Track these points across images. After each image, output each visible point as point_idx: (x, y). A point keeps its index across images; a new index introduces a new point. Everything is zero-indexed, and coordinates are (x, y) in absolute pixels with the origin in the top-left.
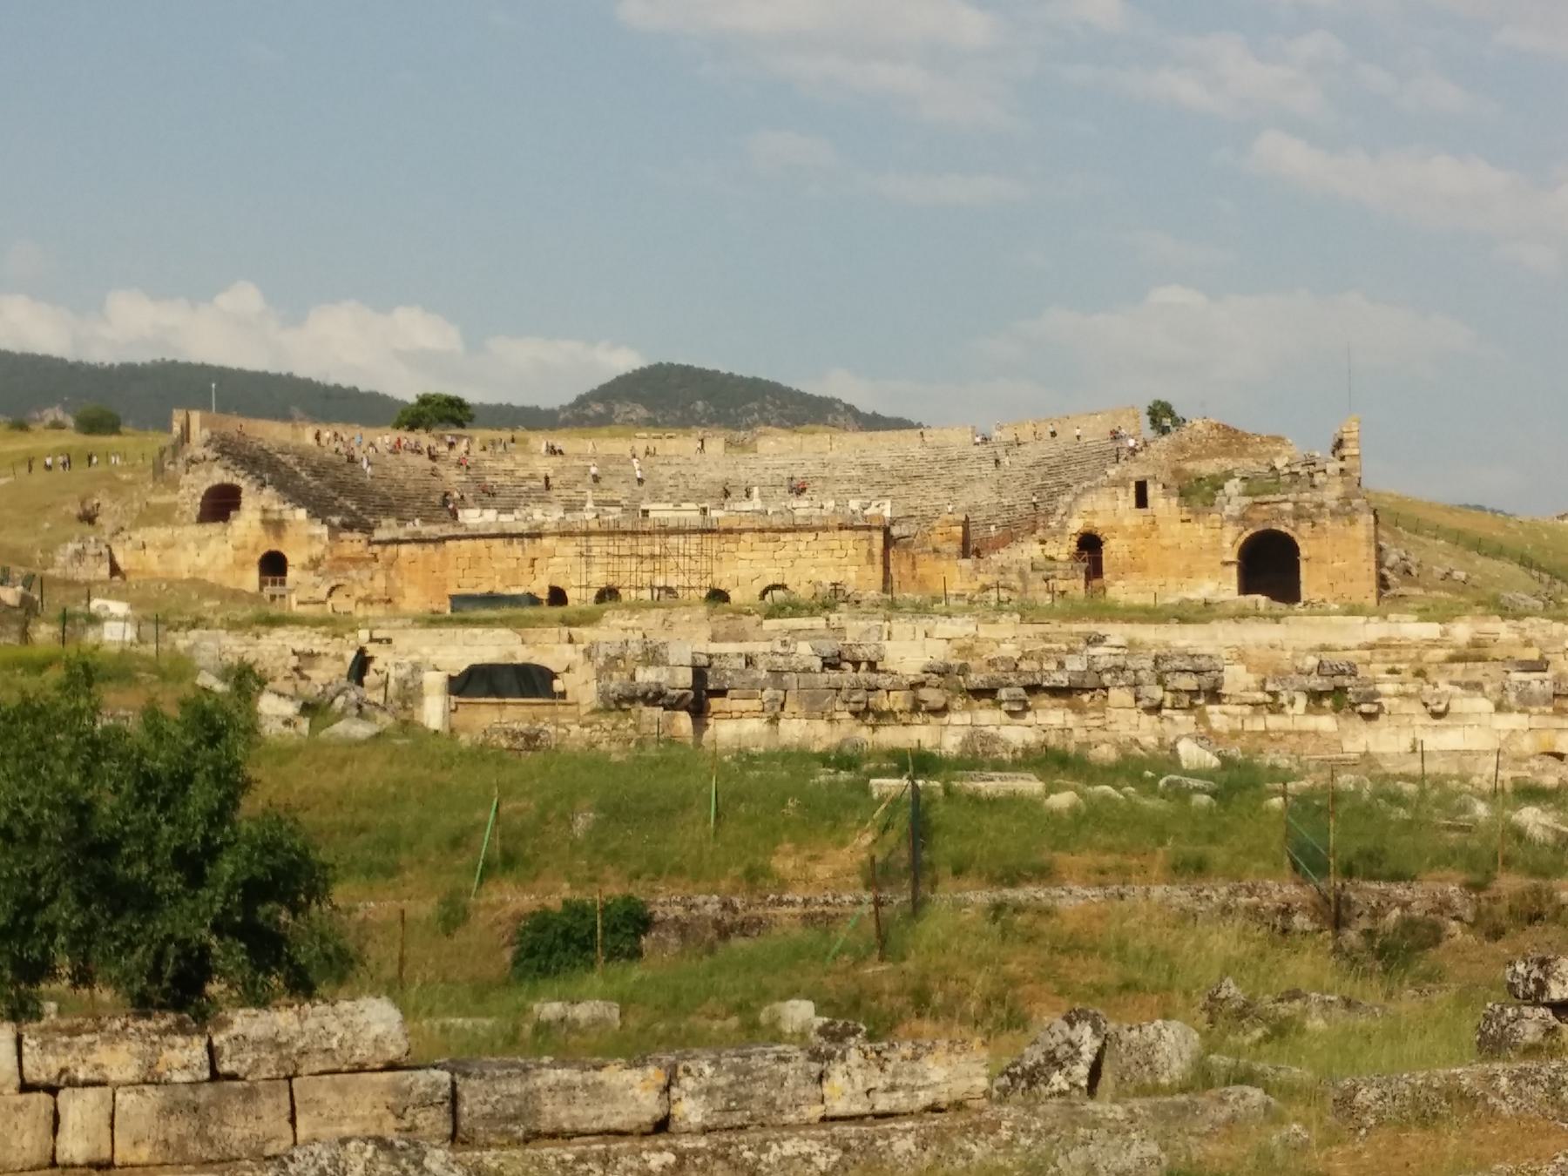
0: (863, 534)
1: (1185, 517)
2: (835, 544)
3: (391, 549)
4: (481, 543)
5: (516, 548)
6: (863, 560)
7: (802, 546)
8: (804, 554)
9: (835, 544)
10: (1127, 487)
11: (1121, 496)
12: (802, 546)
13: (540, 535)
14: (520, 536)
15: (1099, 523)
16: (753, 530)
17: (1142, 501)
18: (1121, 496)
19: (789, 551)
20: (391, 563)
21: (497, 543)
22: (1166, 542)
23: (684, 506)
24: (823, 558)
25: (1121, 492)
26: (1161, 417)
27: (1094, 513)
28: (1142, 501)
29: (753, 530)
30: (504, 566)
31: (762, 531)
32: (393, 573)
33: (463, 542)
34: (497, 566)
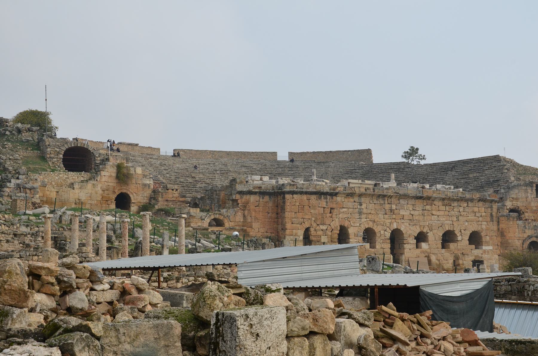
0: (487, 205)
2: (476, 209)
4: (305, 197)
5: (323, 202)
6: (489, 219)
7: (461, 209)
8: (462, 213)
9: (476, 209)
10: (532, 187)
12: (461, 209)
18: (530, 191)
19: (455, 212)
20: (245, 206)
21: (313, 197)
24: (471, 217)
27: (517, 199)
30: (317, 212)
31: (443, 199)
32: (246, 212)
33: (295, 196)
34: (312, 211)
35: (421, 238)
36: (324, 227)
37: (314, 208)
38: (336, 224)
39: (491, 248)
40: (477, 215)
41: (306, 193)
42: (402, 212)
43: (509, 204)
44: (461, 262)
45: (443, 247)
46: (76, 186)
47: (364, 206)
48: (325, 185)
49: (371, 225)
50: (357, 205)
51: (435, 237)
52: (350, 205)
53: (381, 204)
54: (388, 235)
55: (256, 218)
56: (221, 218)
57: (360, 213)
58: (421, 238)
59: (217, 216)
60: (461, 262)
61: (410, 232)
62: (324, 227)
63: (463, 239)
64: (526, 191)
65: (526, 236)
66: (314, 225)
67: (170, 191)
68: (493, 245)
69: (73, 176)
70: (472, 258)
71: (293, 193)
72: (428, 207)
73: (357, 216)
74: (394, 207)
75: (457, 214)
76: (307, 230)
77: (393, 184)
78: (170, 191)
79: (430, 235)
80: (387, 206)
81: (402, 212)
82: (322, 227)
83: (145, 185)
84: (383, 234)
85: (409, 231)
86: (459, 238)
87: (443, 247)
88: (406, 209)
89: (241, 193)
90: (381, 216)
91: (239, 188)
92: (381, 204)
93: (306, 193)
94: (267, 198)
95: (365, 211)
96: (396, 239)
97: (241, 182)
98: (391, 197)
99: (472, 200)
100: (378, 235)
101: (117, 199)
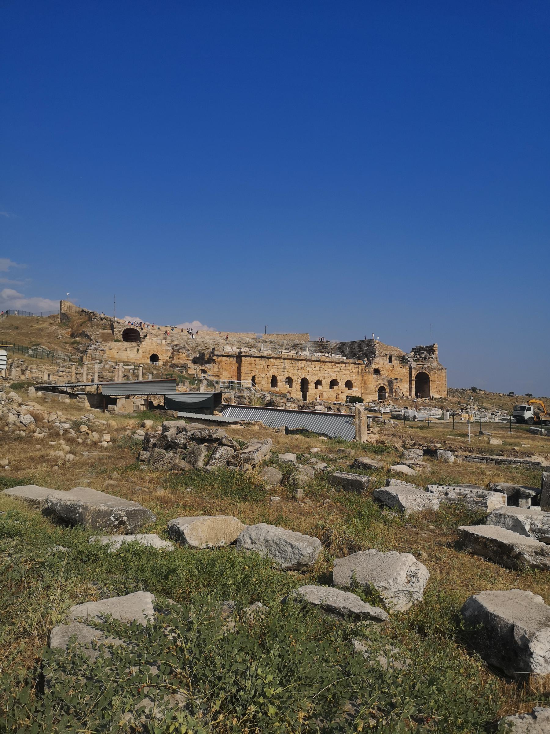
0: (356, 366)
1: (401, 366)
2: (350, 368)
3: (220, 358)
4: (253, 359)
5: (263, 362)
11: (385, 359)
12: (342, 368)
13: (271, 358)
14: (265, 357)
15: (380, 367)
16: (330, 362)
17: (390, 361)
18: (385, 359)
21: (257, 359)
22: (396, 373)
23: (292, 352)
24: (347, 372)
25: (385, 358)
26: (192, 330)
27: (378, 363)
28: (390, 361)
29: (330, 362)
31: (332, 362)
32: (220, 366)
35: (318, 383)
36: (263, 376)
37: (258, 365)
38: (270, 374)
39: (357, 389)
40: (351, 371)
41: (254, 357)
42: (308, 369)
43: (374, 366)
44: (340, 396)
45: (331, 388)
46: (128, 350)
47: (286, 365)
48: (265, 353)
49: (290, 375)
50: (282, 364)
51: (326, 383)
52: (279, 364)
53: (296, 364)
54: (300, 381)
55: (225, 370)
56: (205, 369)
57: (284, 369)
58: (318, 383)
59: (203, 368)
60: (340, 396)
61: (312, 380)
62: (263, 376)
63: (342, 384)
64: (383, 359)
65: (378, 383)
66: (258, 374)
67: (181, 354)
68: (358, 388)
69: (127, 344)
70: (347, 395)
71: (246, 356)
72: (323, 366)
73: (282, 370)
74: (303, 366)
75: (339, 370)
76: (254, 377)
77: (307, 353)
78: (181, 354)
79: (323, 382)
80: (300, 366)
81: (308, 369)
82: (262, 375)
83: (167, 350)
84: (297, 381)
85: (312, 380)
86: (340, 384)
87: (331, 388)
88: (310, 367)
89: (217, 356)
90: (296, 371)
91: (216, 353)
92: (296, 364)
93: (254, 357)
94: (232, 359)
95: (287, 367)
96: (304, 383)
97: (218, 350)
98: (302, 360)
99: (348, 363)
100: (294, 381)
101: (151, 357)
